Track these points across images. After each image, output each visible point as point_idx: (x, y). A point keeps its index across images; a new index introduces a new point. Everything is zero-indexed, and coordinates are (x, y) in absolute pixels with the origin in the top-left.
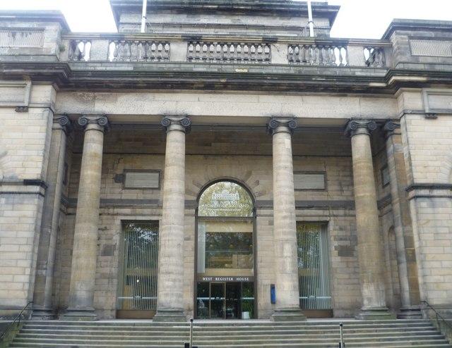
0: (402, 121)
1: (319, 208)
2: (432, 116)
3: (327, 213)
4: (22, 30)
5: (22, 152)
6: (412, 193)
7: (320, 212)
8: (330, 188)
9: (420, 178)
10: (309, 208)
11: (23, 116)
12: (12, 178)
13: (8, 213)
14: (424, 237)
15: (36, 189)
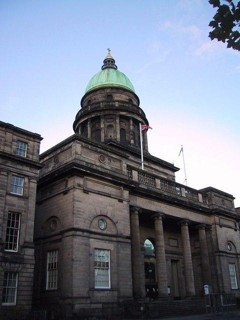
0: (213, 226)
1: (177, 254)
2: (221, 226)
3: (179, 257)
4: (114, 158)
5: (122, 222)
6: (217, 254)
7: (177, 256)
8: (179, 246)
9: (220, 250)
10: (175, 254)
11: (120, 204)
12: (122, 234)
13: (121, 251)
14: (223, 270)
15: (129, 241)
